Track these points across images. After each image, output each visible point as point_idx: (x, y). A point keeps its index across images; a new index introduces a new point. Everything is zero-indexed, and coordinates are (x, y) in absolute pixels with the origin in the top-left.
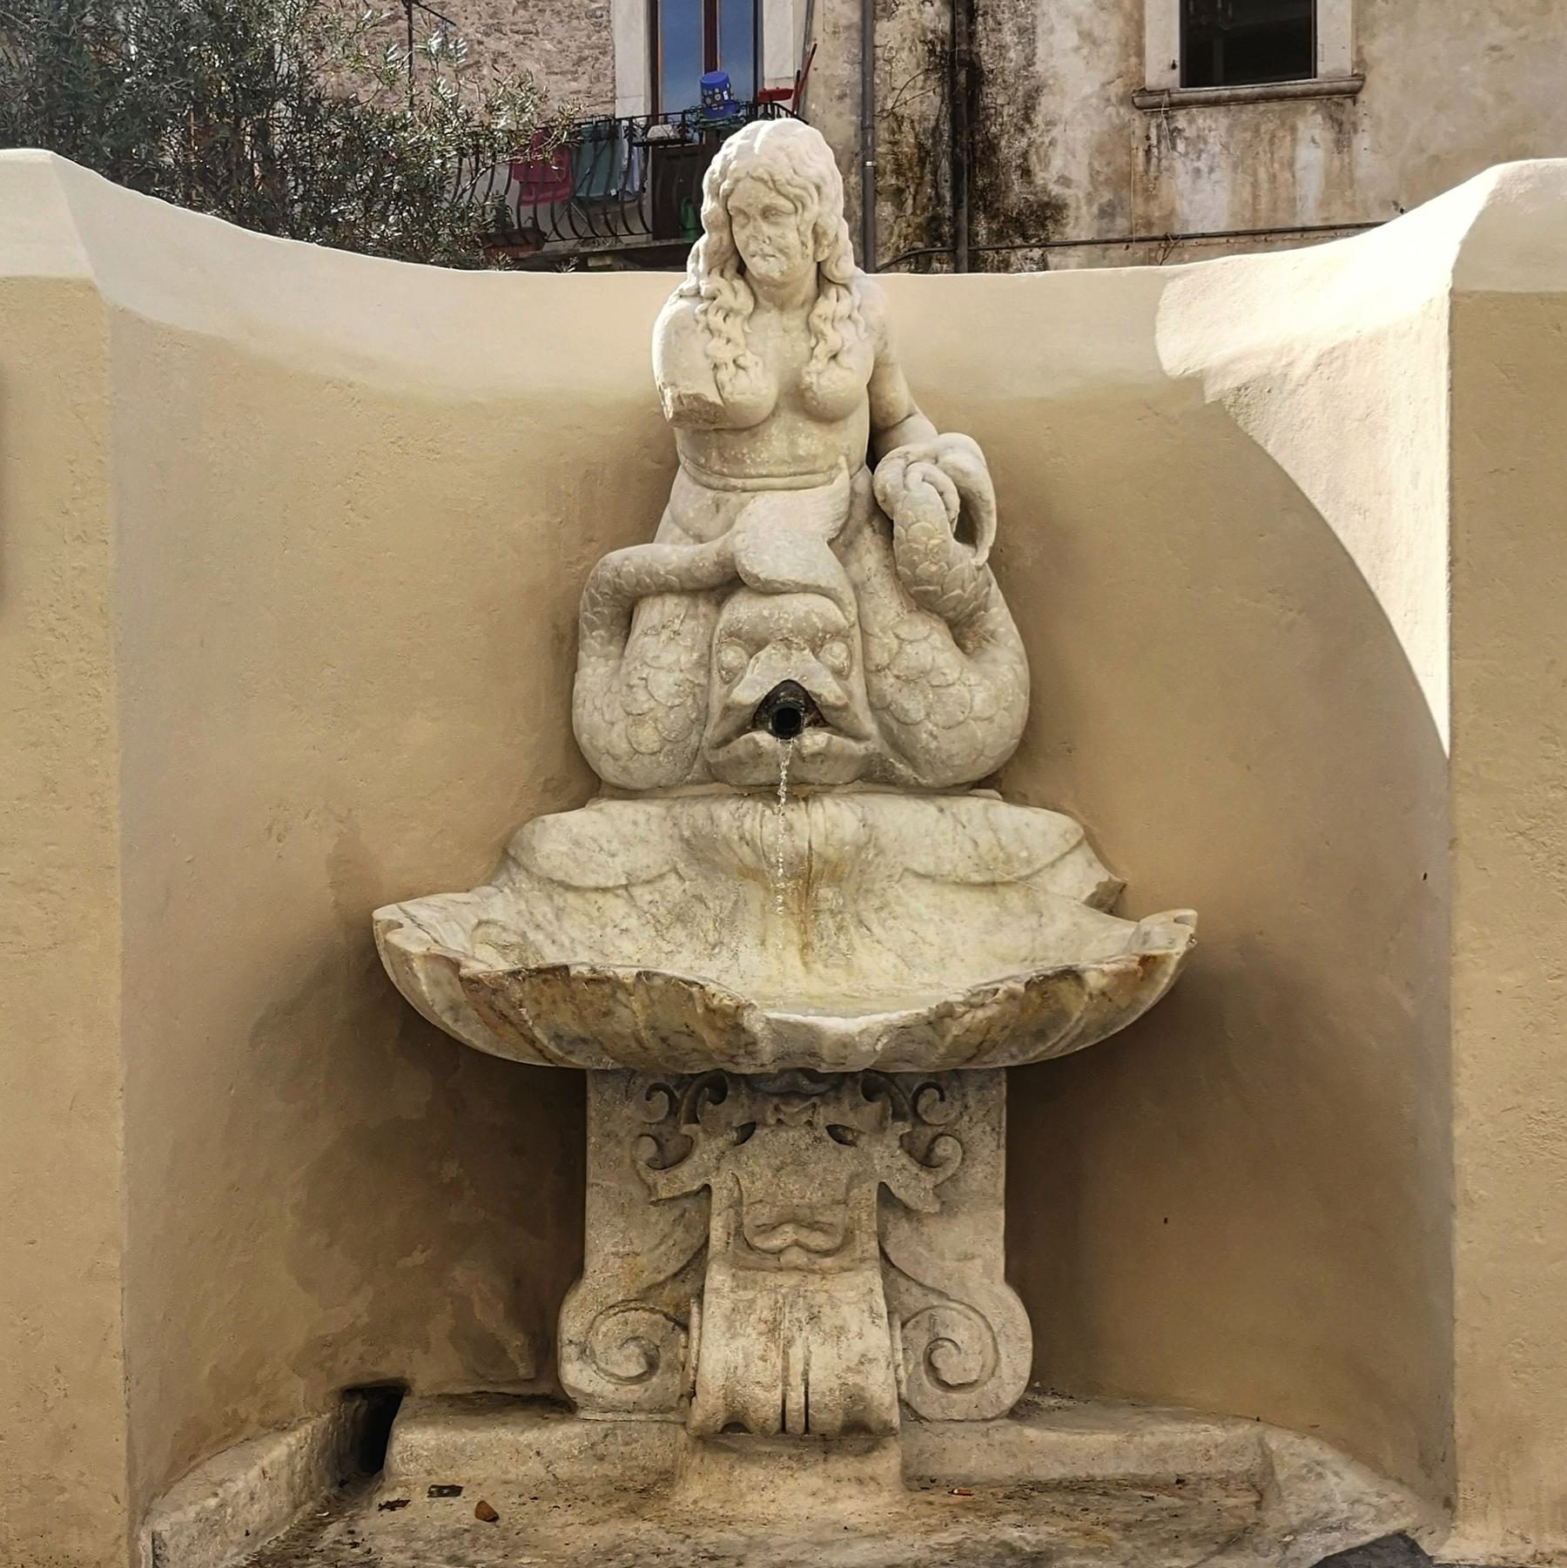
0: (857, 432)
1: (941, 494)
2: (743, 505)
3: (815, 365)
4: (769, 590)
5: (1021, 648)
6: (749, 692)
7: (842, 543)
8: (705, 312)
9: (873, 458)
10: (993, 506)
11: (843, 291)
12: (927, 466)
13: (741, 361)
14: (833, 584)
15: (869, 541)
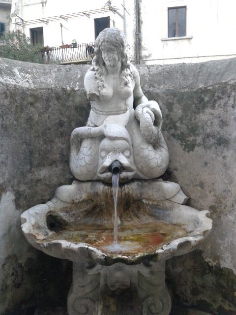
0: (131, 101)
1: (150, 116)
2: (106, 118)
3: (122, 86)
4: (113, 139)
5: (167, 148)
6: (107, 162)
7: (128, 127)
8: (95, 74)
9: (135, 107)
10: (161, 116)
11: (128, 69)
12: (146, 109)
13: (105, 85)
14: (126, 137)
15: (134, 125)
